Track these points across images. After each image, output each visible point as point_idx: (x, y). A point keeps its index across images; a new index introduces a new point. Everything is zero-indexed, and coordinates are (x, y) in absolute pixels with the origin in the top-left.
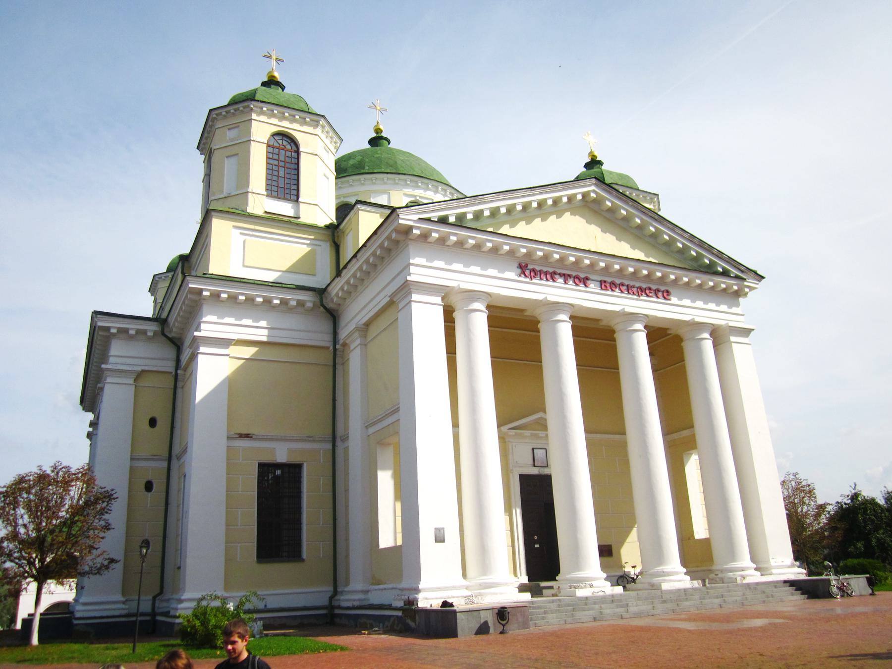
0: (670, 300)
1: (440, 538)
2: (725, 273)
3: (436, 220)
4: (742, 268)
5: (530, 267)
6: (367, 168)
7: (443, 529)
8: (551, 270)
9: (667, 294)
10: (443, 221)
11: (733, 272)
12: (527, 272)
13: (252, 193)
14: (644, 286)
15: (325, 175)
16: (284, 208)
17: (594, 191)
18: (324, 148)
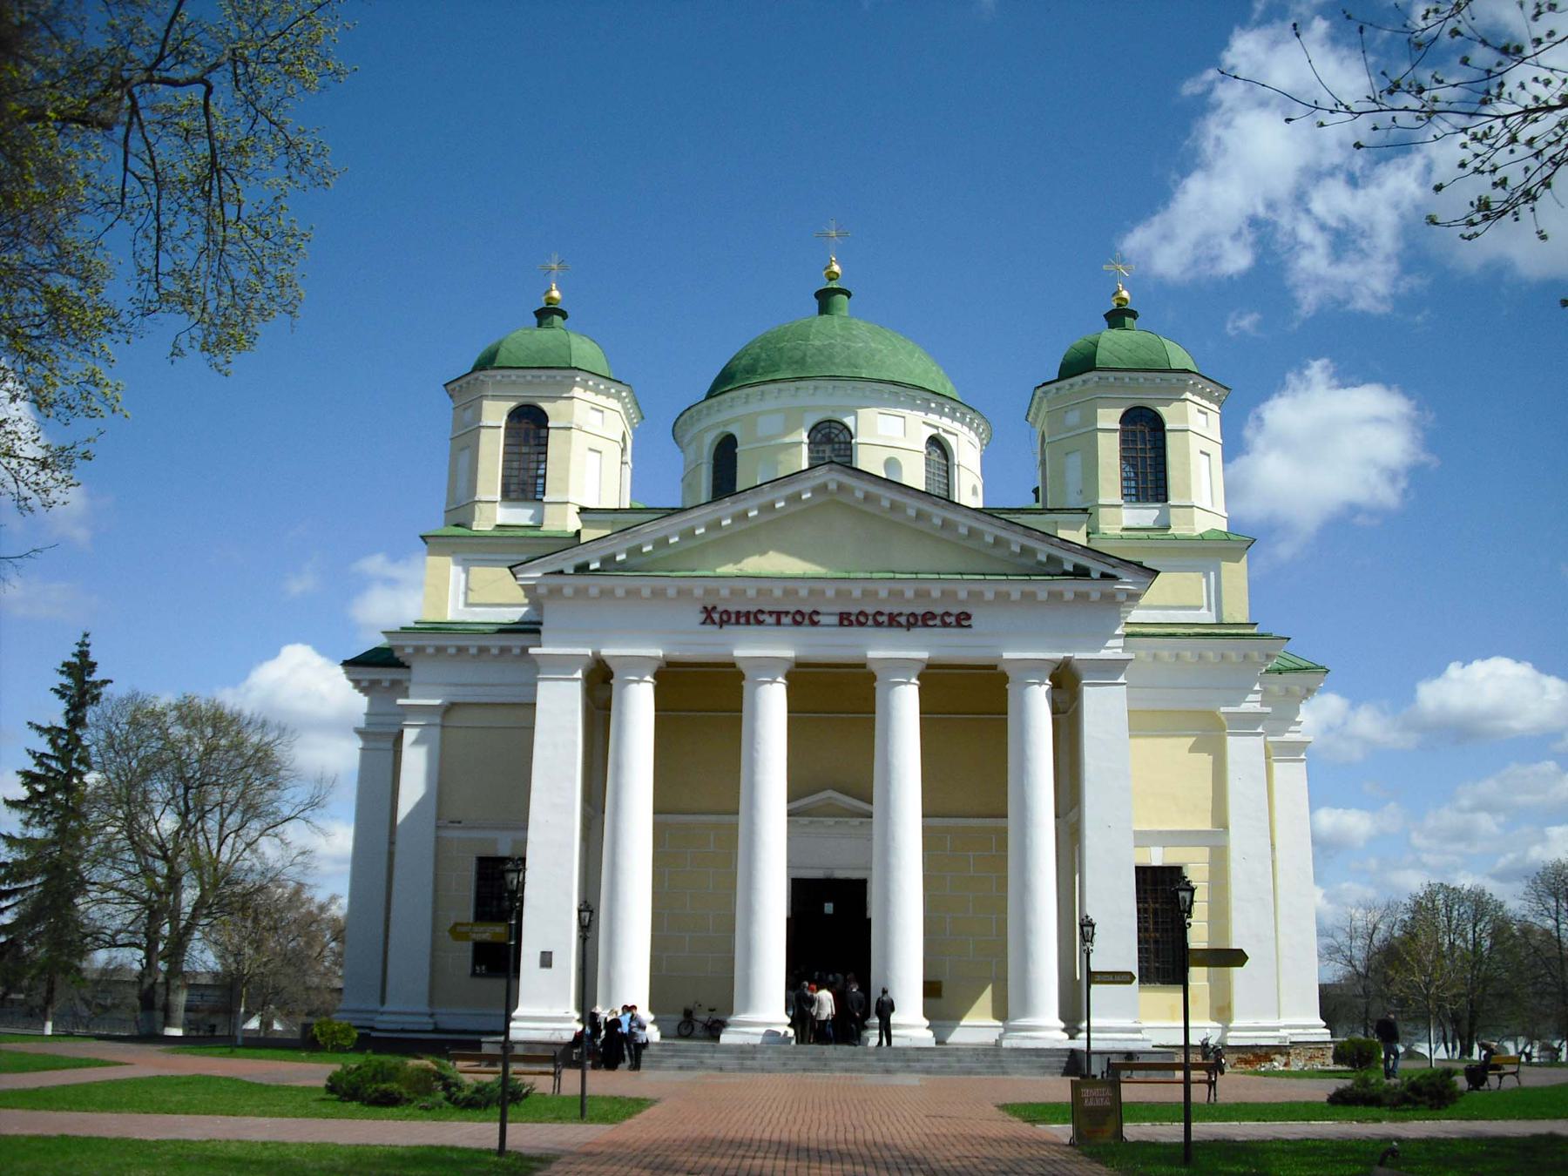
0: (969, 626)
1: (546, 960)
2: (1081, 573)
3: (572, 572)
4: (1112, 561)
5: (720, 609)
6: (760, 371)
7: (551, 953)
8: (754, 609)
9: (963, 620)
10: (582, 569)
11: (1096, 568)
12: (716, 617)
13: (480, 501)
14: (920, 611)
15: (591, 450)
16: (520, 515)
17: (833, 480)
18: (593, 408)
